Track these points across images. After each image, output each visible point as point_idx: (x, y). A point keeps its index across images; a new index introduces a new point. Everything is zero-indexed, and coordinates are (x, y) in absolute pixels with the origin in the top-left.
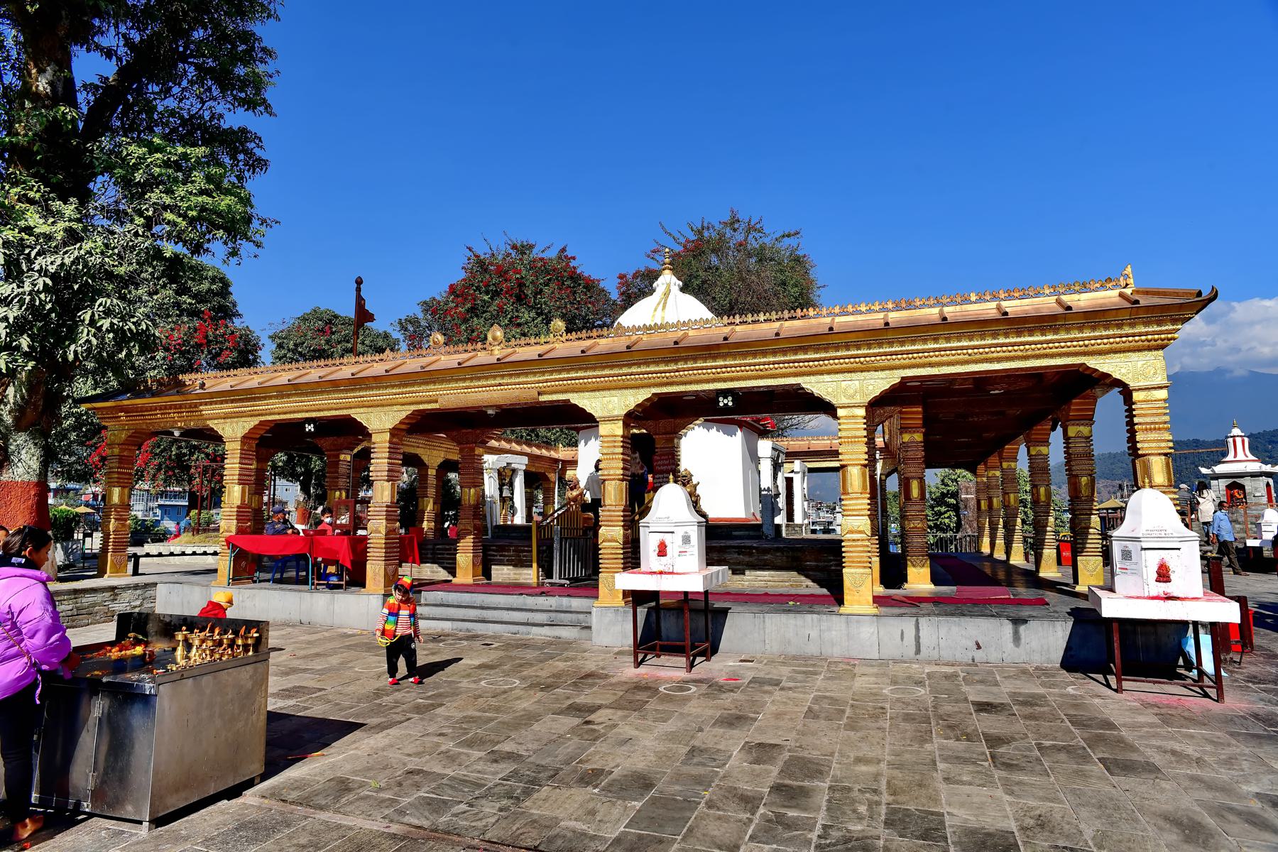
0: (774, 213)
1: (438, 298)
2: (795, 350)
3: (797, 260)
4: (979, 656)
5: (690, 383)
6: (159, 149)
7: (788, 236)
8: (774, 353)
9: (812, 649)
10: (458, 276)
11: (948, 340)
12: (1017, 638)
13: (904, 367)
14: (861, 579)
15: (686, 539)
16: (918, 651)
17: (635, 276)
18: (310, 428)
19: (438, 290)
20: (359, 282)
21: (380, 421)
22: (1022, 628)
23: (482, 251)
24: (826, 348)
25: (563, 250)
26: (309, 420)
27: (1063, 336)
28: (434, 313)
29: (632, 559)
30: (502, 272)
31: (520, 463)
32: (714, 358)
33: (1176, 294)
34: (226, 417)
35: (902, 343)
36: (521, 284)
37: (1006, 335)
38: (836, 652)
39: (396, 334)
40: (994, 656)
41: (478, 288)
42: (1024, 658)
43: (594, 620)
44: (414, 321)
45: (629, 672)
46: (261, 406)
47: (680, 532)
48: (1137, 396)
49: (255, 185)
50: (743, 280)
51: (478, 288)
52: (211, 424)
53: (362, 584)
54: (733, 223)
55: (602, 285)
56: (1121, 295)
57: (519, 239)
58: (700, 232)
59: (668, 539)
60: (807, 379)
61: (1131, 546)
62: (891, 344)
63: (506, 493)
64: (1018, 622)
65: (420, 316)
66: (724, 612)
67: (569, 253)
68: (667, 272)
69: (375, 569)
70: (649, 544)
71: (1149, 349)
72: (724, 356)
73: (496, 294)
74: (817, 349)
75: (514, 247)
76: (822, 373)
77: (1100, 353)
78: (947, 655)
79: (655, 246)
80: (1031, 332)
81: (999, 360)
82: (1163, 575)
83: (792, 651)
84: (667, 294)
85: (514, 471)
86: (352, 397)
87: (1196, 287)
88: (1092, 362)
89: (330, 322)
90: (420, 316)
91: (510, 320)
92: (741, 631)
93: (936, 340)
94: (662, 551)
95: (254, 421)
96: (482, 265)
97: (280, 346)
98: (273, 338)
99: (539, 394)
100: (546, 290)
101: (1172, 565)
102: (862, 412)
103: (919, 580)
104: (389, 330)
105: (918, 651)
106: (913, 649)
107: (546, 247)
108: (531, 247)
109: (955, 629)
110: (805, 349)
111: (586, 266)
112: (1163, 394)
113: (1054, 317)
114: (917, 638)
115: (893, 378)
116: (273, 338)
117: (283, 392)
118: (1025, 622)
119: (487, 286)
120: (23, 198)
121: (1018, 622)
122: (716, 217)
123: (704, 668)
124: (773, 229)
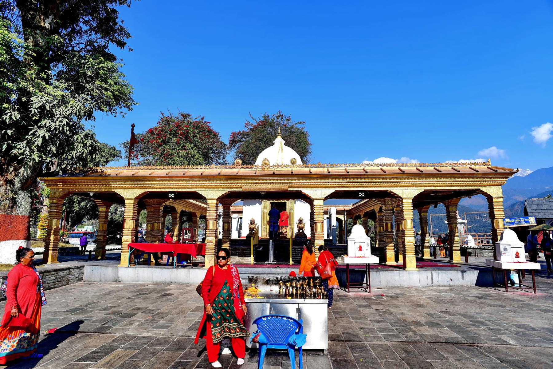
3: (302, 133)
4: (452, 283)
5: (350, 187)
7: (300, 123)
8: (383, 179)
9: (397, 284)
10: (154, 124)
11: (440, 178)
13: (424, 186)
15: (368, 245)
16: (432, 283)
17: (238, 133)
20: (133, 126)
22: (464, 274)
23: (167, 114)
25: (203, 119)
30: (178, 126)
32: (361, 178)
33: (506, 169)
35: (426, 178)
36: (188, 133)
37: (458, 178)
46: (148, 184)
48: (494, 200)
52: (116, 191)
54: (280, 116)
56: (488, 168)
57: (185, 112)
59: (362, 244)
60: (393, 188)
61: (507, 247)
64: (463, 272)
68: (279, 137)
71: (498, 186)
72: (365, 178)
73: (175, 135)
74: (397, 178)
75: (182, 115)
76: (397, 187)
78: (442, 284)
82: (517, 256)
83: (390, 284)
87: (511, 168)
91: (182, 147)
95: (143, 191)
96: (167, 121)
99: (289, 187)
102: (411, 201)
105: (432, 283)
106: (430, 283)
107: (195, 117)
108: (190, 116)
109: (444, 275)
110: (393, 178)
111: (214, 128)
112: (501, 200)
113: (470, 174)
114: (432, 278)
117: (161, 178)
118: (465, 272)
121: (463, 272)
122: (272, 113)
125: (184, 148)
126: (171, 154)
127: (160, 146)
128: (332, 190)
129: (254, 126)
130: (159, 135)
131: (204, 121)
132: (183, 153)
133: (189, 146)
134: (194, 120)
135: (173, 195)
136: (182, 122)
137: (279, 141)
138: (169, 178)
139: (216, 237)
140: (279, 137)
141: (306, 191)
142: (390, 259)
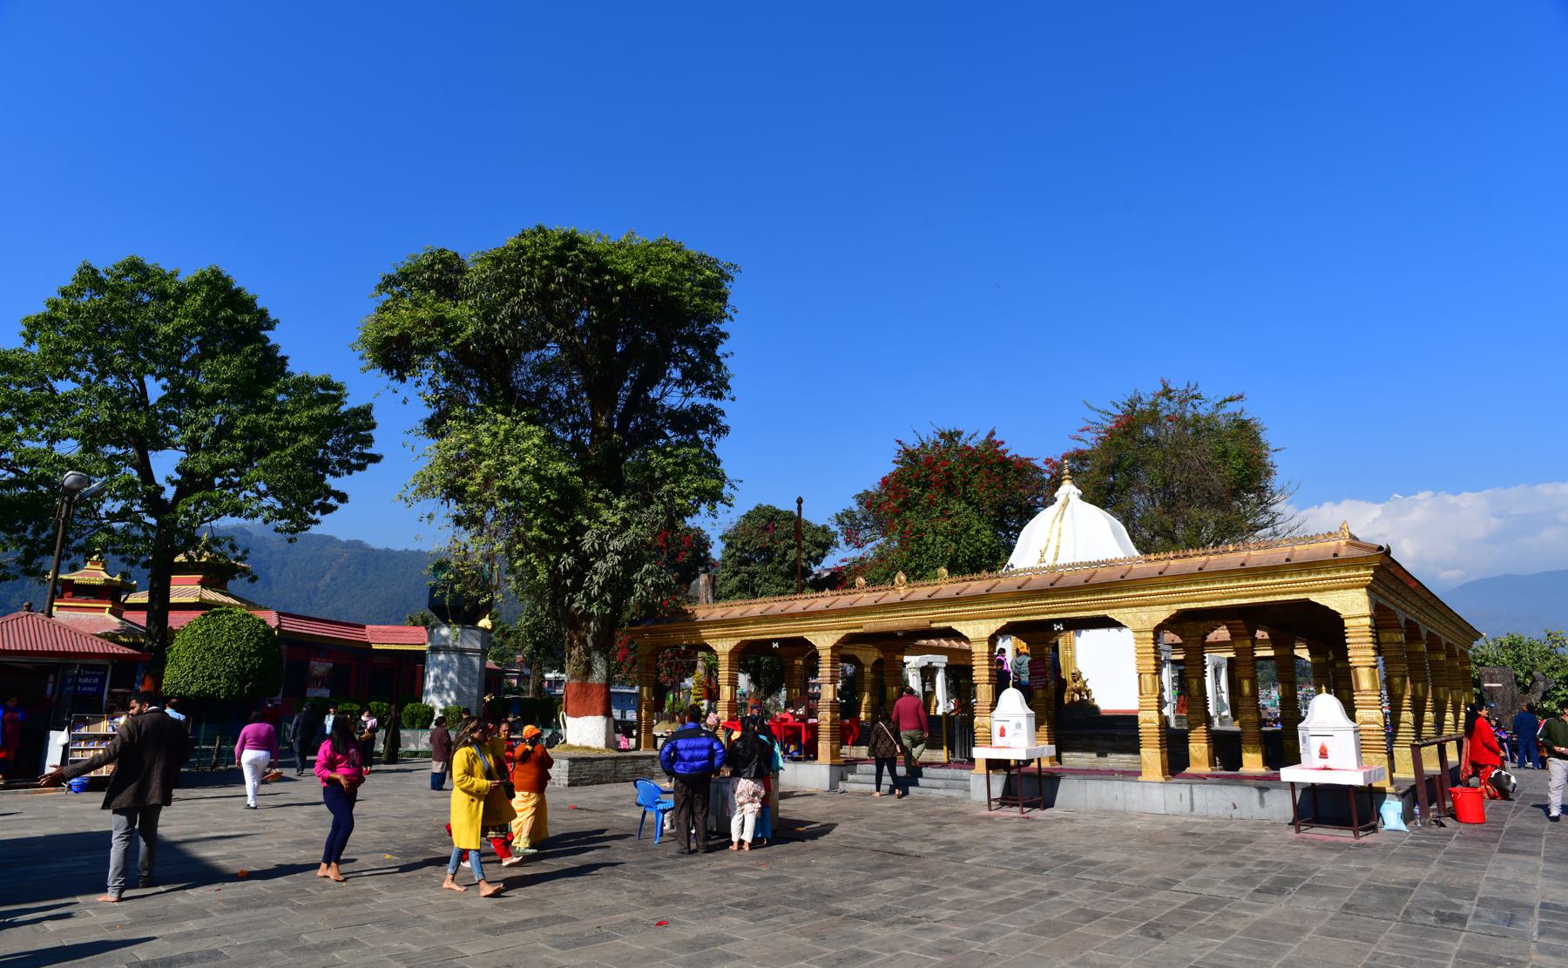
0: (1214, 376)
1: (871, 490)
2: (1101, 592)
3: (1243, 426)
4: (1236, 813)
6: (670, 455)
9: (1119, 806)
12: (1262, 801)
15: (1019, 726)
16: (1192, 809)
18: (776, 645)
19: (872, 484)
21: (824, 641)
22: (1266, 794)
23: (912, 443)
24: (1121, 590)
25: (992, 433)
26: (775, 640)
27: (1287, 579)
28: (868, 507)
30: (930, 463)
31: (940, 661)
34: (718, 637)
36: (949, 476)
39: (834, 528)
40: (1246, 815)
41: (909, 482)
42: (1267, 816)
43: (972, 784)
44: (849, 514)
45: (985, 812)
47: (1014, 721)
49: (722, 448)
51: (909, 482)
52: (707, 642)
53: (816, 758)
54: (1167, 393)
57: (948, 427)
58: (1132, 405)
62: (1166, 586)
63: (928, 688)
65: (856, 508)
66: (1059, 779)
67: (997, 438)
69: (824, 747)
72: (1053, 597)
73: (926, 486)
77: (1319, 591)
78: (1212, 812)
79: (1085, 425)
80: (1265, 576)
81: (1246, 597)
82: (1323, 754)
83: (1105, 807)
85: (936, 669)
86: (804, 625)
88: (1314, 598)
89: (771, 519)
90: (856, 508)
92: (1068, 792)
93: (1197, 583)
94: (1002, 734)
95: (736, 641)
96: (909, 454)
97: (729, 546)
98: (722, 538)
101: (1328, 747)
102: (1151, 635)
104: (828, 523)
105: (1192, 809)
107: (974, 435)
108: (959, 434)
110: (1107, 591)
114: (1192, 800)
116: (722, 538)
117: (757, 620)
118: (1267, 789)
119: (917, 478)
120: (596, 499)
122: (1148, 389)
123: (1037, 813)
126: (920, 531)
128: (1001, 623)
133: (957, 506)
135: (776, 645)
136: (947, 449)
137: (1068, 490)
139: (1160, 712)
140: (1067, 482)
142: (1198, 761)
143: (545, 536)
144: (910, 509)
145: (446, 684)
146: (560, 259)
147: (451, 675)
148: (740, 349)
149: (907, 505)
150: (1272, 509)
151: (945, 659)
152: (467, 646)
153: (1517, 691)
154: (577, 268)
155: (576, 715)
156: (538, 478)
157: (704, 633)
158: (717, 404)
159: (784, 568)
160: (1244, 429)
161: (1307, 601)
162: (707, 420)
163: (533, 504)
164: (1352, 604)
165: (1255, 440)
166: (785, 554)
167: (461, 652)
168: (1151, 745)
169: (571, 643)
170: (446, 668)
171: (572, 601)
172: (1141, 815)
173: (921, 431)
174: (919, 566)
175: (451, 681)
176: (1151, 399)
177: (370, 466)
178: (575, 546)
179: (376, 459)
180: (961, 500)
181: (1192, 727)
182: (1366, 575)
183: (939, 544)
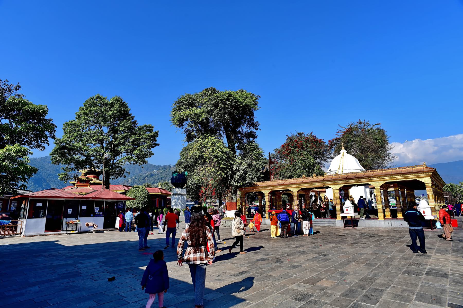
3: (380, 131)
4: (402, 226)
9: (374, 226)
14: (380, 214)
15: (351, 209)
17: (333, 140)
19: (279, 147)
21: (295, 191)
23: (290, 136)
25: (312, 133)
29: (342, 211)
30: (296, 141)
36: (303, 145)
38: (378, 226)
40: (404, 226)
45: (344, 228)
46: (272, 188)
47: (350, 207)
50: (363, 139)
55: (324, 141)
57: (300, 131)
65: (274, 153)
70: (345, 209)
73: (296, 147)
75: (299, 134)
78: (396, 226)
83: (370, 226)
84: (343, 155)
88: (418, 179)
90: (274, 153)
94: (347, 210)
100: (309, 146)
103: (400, 216)
107: (306, 134)
111: (319, 137)
115: (385, 182)
117: (276, 186)
122: (355, 122)
124: (372, 123)
125: (301, 155)
126: (295, 159)
127: (288, 155)
129: (345, 133)
130: (287, 149)
131: (312, 134)
132: (302, 157)
133: (304, 153)
134: (306, 136)
137: (343, 151)
138: (278, 185)
141: (330, 186)
142: (387, 216)
143: (224, 166)
144: (291, 154)
145: (178, 203)
146: (228, 100)
147: (179, 201)
148: (258, 116)
149: (290, 152)
150: (388, 152)
151: (314, 193)
152: (183, 193)
153: (453, 198)
154: (231, 102)
155: (230, 210)
156: (222, 152)
157: (261, 189)
158: (256, 131)
159: (255, 170)
160: (381, 131)
161: (417, 180)
162: (252, 135)
163: (222, 159)
164: (427, 181)
165: (383, 134)
166: (255, 166)
167: (181, 195)
168: (381, 212)
169: (227, 192)
170: (178, 199)
171: (230, 182)
172: (380, 227)
173: (293, 132)
174: (295, 169)
175: (179, 203)
176: (355, 124)
177: (157, 146)
178: (232, 169)
179: (158, 145)
180: (308, 152)
181: (386, 208)
182: (430, 174)
183: (300, 163)
